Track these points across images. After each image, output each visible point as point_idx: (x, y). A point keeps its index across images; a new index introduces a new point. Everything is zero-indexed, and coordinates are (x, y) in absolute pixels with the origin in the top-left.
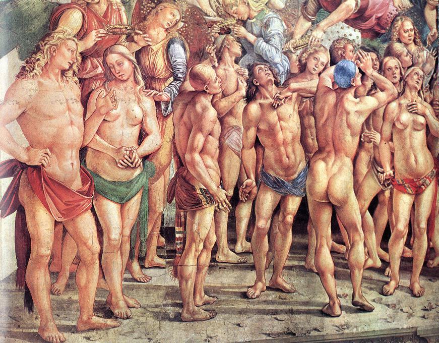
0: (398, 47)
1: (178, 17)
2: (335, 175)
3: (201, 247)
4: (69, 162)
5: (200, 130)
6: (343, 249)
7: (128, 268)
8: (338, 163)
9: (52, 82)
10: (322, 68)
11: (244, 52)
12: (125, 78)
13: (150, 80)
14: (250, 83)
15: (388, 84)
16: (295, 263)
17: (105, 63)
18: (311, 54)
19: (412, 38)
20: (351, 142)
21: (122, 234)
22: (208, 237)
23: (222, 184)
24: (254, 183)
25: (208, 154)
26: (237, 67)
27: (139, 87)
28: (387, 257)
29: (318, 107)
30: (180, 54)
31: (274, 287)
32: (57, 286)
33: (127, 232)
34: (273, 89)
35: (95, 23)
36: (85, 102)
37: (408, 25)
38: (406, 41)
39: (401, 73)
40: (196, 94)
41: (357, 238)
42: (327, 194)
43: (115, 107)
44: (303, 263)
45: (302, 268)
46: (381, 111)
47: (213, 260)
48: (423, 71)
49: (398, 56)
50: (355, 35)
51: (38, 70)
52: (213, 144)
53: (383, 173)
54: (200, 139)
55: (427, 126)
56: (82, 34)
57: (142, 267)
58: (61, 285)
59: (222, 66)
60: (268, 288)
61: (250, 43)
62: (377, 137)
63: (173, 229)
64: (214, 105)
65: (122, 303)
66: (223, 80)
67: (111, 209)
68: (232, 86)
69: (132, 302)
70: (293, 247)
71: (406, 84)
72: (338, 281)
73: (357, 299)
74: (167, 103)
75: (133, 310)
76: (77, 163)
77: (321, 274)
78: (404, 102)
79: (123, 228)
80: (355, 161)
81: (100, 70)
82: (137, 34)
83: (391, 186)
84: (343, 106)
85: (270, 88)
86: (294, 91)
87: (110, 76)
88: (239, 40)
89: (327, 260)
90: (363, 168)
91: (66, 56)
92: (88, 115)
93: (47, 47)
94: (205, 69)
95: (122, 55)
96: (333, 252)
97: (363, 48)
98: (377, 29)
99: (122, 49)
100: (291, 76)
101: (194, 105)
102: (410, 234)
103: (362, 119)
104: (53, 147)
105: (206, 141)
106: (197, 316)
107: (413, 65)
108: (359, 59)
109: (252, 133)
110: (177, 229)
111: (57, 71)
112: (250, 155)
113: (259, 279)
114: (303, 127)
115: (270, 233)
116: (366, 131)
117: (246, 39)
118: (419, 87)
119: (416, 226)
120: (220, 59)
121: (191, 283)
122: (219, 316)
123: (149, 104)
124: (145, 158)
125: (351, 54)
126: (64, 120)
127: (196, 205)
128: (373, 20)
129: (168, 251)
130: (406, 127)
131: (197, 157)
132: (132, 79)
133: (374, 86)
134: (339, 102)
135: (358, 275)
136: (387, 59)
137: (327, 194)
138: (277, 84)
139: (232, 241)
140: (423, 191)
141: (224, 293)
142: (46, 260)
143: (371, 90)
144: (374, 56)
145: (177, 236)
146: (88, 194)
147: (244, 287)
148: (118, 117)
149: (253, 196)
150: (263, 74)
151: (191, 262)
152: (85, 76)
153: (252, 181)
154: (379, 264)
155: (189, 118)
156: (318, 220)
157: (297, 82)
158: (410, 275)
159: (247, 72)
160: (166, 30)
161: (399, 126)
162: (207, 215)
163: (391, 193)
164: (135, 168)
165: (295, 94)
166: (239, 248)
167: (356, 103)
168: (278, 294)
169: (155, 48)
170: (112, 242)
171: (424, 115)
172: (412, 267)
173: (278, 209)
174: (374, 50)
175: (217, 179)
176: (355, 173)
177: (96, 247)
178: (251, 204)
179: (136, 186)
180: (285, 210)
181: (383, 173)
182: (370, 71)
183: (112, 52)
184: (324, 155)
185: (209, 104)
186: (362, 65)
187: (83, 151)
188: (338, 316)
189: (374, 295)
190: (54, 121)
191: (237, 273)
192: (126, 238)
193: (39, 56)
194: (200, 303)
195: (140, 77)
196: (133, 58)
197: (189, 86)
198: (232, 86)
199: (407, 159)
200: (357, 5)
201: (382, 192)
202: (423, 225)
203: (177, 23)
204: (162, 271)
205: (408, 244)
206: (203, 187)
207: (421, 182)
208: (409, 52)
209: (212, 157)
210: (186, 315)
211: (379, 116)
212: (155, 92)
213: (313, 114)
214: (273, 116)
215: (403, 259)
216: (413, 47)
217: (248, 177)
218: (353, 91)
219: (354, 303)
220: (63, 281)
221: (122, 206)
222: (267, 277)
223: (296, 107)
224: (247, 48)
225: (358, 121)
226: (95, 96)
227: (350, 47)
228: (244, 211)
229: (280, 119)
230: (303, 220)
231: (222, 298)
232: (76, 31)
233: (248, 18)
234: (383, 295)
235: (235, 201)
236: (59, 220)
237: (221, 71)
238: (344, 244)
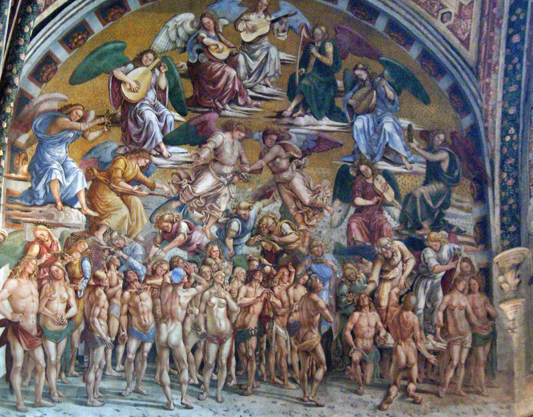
0: (210, 260)
1: (87, 247)
2: (171, 332)
3: (97, 366)
4: (31, 321)
5: (97, 305)
6: (176, 372)
7: (60, 376)
8: (173, 325)
9: (24, 280)
10: (165, 272)
11: (122, 264)
12: (60, 278)
13: (73, 279)
14: (125, 280)
15: (204, 281)
16: (148, 379)
17: (50, 271)
18: (159, 265)
19: (218, 255)
20: (181, 313)
21: (57, 358)
22: (101, 362)
23: (109, 333)
24: (126, 334)
25: (101, 318)
26: (117, 272)
27: (66, 283)
28: (202, 379)
29: (163, 293)
30: (87, 265)
31: (136, 391)
32: (24, 383)
33: (59, 357)
34: (137, 284)
35: (45, 250)
36: (40, 290)
37: (216, 248)
38: (214, 257)
39: (211, 275)
40: (95, 287)
41: (184, 367)
42: (167, 342)
43: (55, 293)
44: (153, 379)
45: (150, 381)
46: (199, 297)
47: (104, 374)
48: (225, 273)
49: (210, 265)
50: (183, 254)
51: (18, 274)
52: (104, 313)
53: (200, 331)
54: (97, 311)
55: (227, 305)
56: (39, 256)
57: (67, 376)
58: (26, 383)
59: (110, 272)
60: (134, 392)
61: (125, 259)
62: (197, 311)
63: (83, 357)
64: (105, 292)
65: (56, 394)
66: (110, 279)
67: (51, 345)
68: (114, 282)
69: (61, 394)
70: (148, 370)
71: (214, 282)
72: (173, 391)
73: (184, 401)
74: (81, 291)
75: (62, 398)
76: (35, 321)
77: (163, 385)
78: (213, 291)
79: (57, 355)
80: (183, 323)
81: (47, 274)
82: (66, 256)
83: (205, 339)
84: (176, 293)
85: (135, 283)
86: (148, 285)
87: (53, 278)
88: (118, 258)
89: (167, 379)
90: (188, 328)
91: (31, 267)
92: (41, 297)
93: (22, 263)
94: (101, 274)
95: (58, 266)
96: (170, 373)
97: (189, 261)
98: (197, 250)
99: (59, 264)
100: (147, 277)
101: (95, 292)
102: (216, 367)
103: (188, 300)
104: (24, 313)
105: (101, 311)
106: (94, 404)
107: (219, 270)
108: (186, 267)
109: (125, 307)
110: (85, 357)
111: (27, 275)
112: (124, 319)
113: (128, 386)
114: (154, 305)
115: (135, 361)
116: (190, 307)
117: (122, 257)
118: (222, 283)
119: (219, 362)
120: (109, 268)
121: (92, 386)
122: (106, 405)
123: (71, 292)
124: (70, 319)
125: (181, 265)
126: (30, 299)
127: (96, 346)
128: (194, 246)
129: (80, 368)
130: (214, 305)
131: (96, 320)
132: (63, 279)
133: (196, 282)
134: (174, 291)
135: (185, 388)
136: (203, 267)
137: (167, 342)
138: (139, 281)
139: (114, 364)
140: (224, 342)
141: (109, 393)
142: (20, 369)
143: (194, 284)
144: (195, 266)
145: (85, 360)
146: (40, 337)
147: (120, 390)
148: (55, 298)
149: (125, 342)
150: (132, 276)
151: (91, 376)
152: (41, 277)
153: (125, 333)
154: (197, 382)
155: (92, 299)
156: (161, 356)
157: (151, 280)
158: (216, 390)
159: (123, 275)
160: (81, 253)
161: (210, 305)
162: (102, 349)
163: (205, 343)
164: (64, 325)
165: (149, 287)
166: (118, 368)
167: (184, 292)
168: (139, 395)
169: (75, 263)
170: (53, 363)
171: (225, 299)
172: (217, 386)
173: (140, 349)
174: (194, 262)
175: (106, 331)
176: (183, 331)
177: (44, 365)
178: (124, 346)
179: (64, 334)
180: (143, 349)
181: (200, 331)
182: (193, 274)
183: (54, 265)
184: (165, 320)
185: (102, 292)
186: (188, 271)
187: (38, 315)
188: (172, 410)
189: (195, 400)
190: (24, 300)
191: (117, 382)
192: (59, 361)
193: (19, 267)
194: (96, 397)
195: (67, 278)
196: (64, 269)
197: (92, 283)
198: (114, 282)
199: (214, 323)
200: (185, 238)
201: (199, 342)
202: (224, 362)
203: (86, 250)
204: (76, 379)
205: (215, 372)
206: (99, 335)
207: (224, 337)
208: (216, 263)
209: (103, 319)
210: (89, 403)
211: (198, 299)
212: (75, 285)
213: (160, 297)
214: (137, 298)
215: (212, 380)
216: (218, 260)
217: (123, 331)
218: (183, 285)
219: (182, 404)
220: (28, 380)
221: (57, 345)
222: (133, 385)
223: (150, 293)
224: (123, 261)
225: (184, 301)
226: (45, 287)
227: (181, 261)
228: (121, 349)
229: (141, 300)
230: (154, 355)
231: (108, 395)
232: (36, 255)
233: (125, 246)
234: (199, 399)
235: (116, 344)
236: (26, 349)
237: (109, 275)
238: (177, 370)
